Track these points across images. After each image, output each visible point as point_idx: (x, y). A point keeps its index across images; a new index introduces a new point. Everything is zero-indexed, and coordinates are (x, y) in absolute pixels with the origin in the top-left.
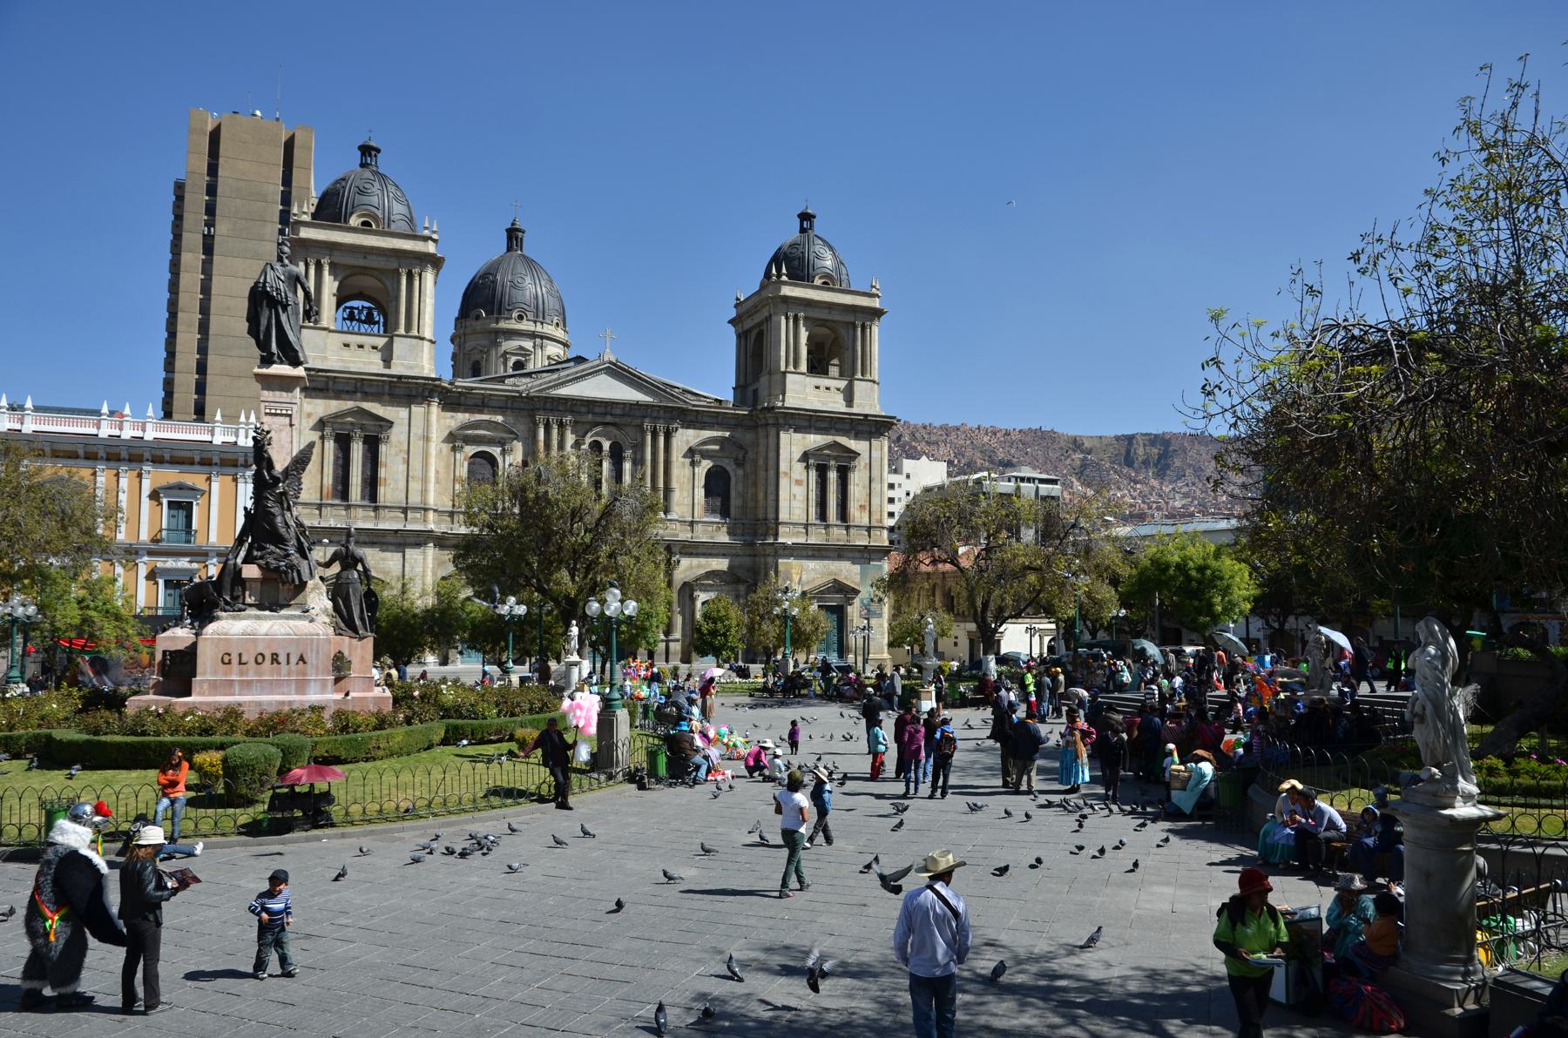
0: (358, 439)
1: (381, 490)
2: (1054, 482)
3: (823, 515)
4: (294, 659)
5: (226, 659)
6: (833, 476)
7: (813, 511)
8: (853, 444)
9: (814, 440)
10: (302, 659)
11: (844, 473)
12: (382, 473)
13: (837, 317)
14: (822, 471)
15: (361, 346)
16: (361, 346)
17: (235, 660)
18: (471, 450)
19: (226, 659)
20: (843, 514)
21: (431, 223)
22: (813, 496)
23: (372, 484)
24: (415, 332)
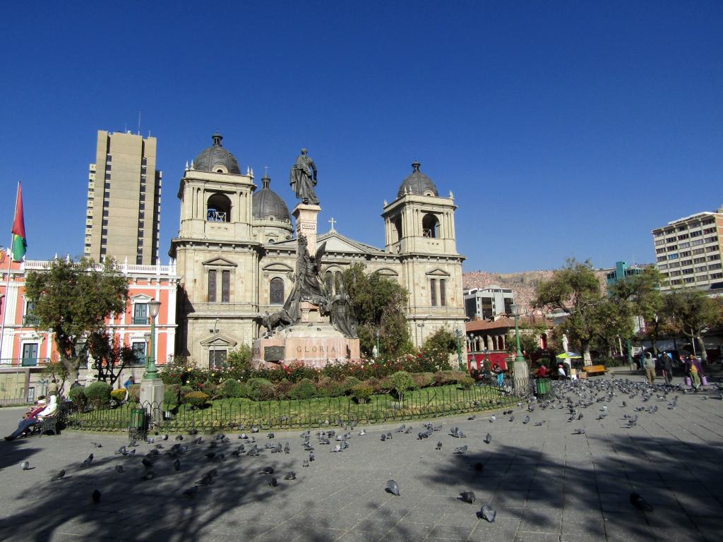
0: (219, 276)
1: (231, 297)
2: (510, 291)
3: (434, 303)
4: (330, 349)
5: (299, 349)
6: (438, 284)
8: (447, 269)
9: (429, 266)
10: (333, 349)
12: (231, 288)
15: (219, 228)
16: (219, 228)
17: (303, 351)
18: (272, 275)
19: (299, 349)
20: (443, 303)
21: (250, 170)
23: (226, 294)
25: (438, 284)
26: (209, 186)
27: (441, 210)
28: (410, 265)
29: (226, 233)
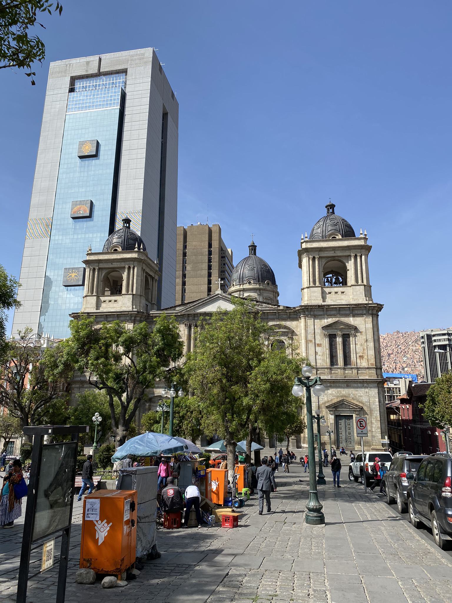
6: (339, 340)
7: (328, 361)
8: (351, 321)
11: (346, 338)
13: (339, 253)
14: (332, 338)
15: (110, 301)
16: (110, 301)
22: (328, 352)
24: (130, 292)
25: (339, 340)
26: (101, 265)
27: (347, 253)
28: (303, 320)
29: (115, 305)
